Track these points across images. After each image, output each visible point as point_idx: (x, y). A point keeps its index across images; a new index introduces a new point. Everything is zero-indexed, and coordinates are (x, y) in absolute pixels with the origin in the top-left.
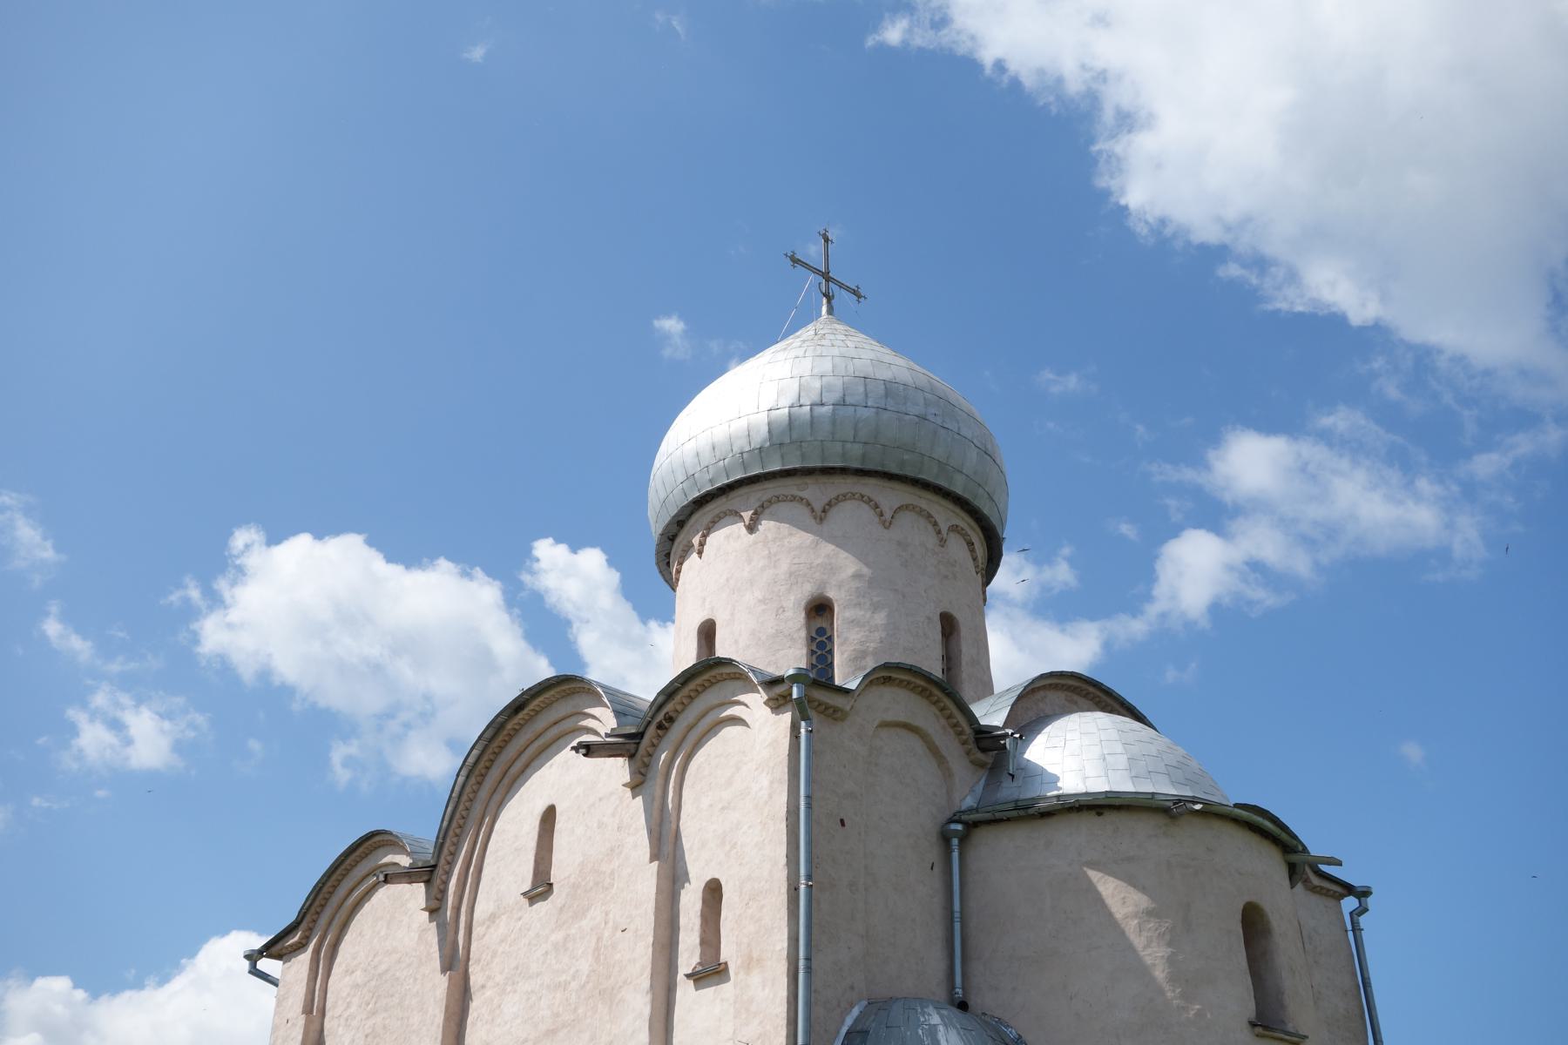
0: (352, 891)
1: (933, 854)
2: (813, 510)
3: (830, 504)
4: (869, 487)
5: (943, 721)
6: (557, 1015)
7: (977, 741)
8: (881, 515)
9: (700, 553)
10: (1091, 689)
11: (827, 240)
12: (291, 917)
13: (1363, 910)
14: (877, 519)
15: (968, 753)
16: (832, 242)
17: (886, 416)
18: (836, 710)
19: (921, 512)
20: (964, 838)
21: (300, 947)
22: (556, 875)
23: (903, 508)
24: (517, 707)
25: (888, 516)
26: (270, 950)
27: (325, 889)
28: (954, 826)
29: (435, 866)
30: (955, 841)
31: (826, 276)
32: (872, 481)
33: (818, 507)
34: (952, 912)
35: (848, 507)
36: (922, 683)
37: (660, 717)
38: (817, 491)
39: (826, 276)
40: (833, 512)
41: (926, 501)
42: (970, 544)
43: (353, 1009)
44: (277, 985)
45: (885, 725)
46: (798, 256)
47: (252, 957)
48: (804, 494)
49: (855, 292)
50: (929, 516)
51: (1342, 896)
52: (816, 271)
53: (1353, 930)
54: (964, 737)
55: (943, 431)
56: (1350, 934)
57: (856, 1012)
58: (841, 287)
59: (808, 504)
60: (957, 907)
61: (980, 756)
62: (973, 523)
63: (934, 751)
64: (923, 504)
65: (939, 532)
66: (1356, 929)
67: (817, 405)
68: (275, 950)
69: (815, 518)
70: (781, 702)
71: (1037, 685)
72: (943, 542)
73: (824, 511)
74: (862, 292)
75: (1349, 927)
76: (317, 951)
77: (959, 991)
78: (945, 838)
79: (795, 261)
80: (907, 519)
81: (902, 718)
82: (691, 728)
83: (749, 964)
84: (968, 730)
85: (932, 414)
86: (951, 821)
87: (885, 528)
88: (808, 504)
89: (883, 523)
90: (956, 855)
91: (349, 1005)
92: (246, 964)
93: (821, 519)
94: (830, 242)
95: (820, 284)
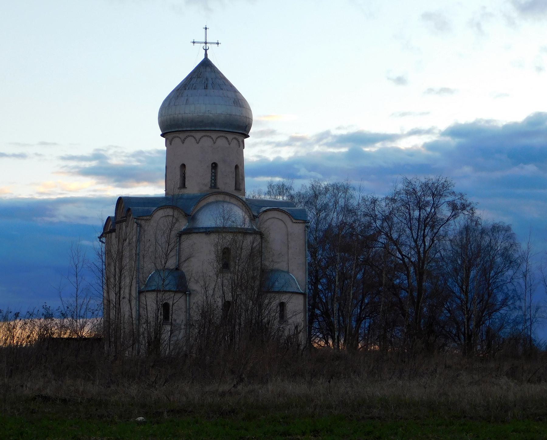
4: (193, 134)
8: (196, 140)
11: (206, 29)
14: (196, 142)
19: (208, 136)
31: (206, 43)
33: (183, 138)
35: (190, 138)
38: (182, 136)
39: (206, 43)
40: (186, 141)
41: (209, 134)
46: (195, 41)
47: (100, 238)
48: (178, 136)
49: (218, 44)
64: (209, 134)
69: (182, 142)
72: (215, 143)
85: (207, 111)
89: (197, 142)
92: (98, 239)
93: (184, 143)
94: (207, 29)
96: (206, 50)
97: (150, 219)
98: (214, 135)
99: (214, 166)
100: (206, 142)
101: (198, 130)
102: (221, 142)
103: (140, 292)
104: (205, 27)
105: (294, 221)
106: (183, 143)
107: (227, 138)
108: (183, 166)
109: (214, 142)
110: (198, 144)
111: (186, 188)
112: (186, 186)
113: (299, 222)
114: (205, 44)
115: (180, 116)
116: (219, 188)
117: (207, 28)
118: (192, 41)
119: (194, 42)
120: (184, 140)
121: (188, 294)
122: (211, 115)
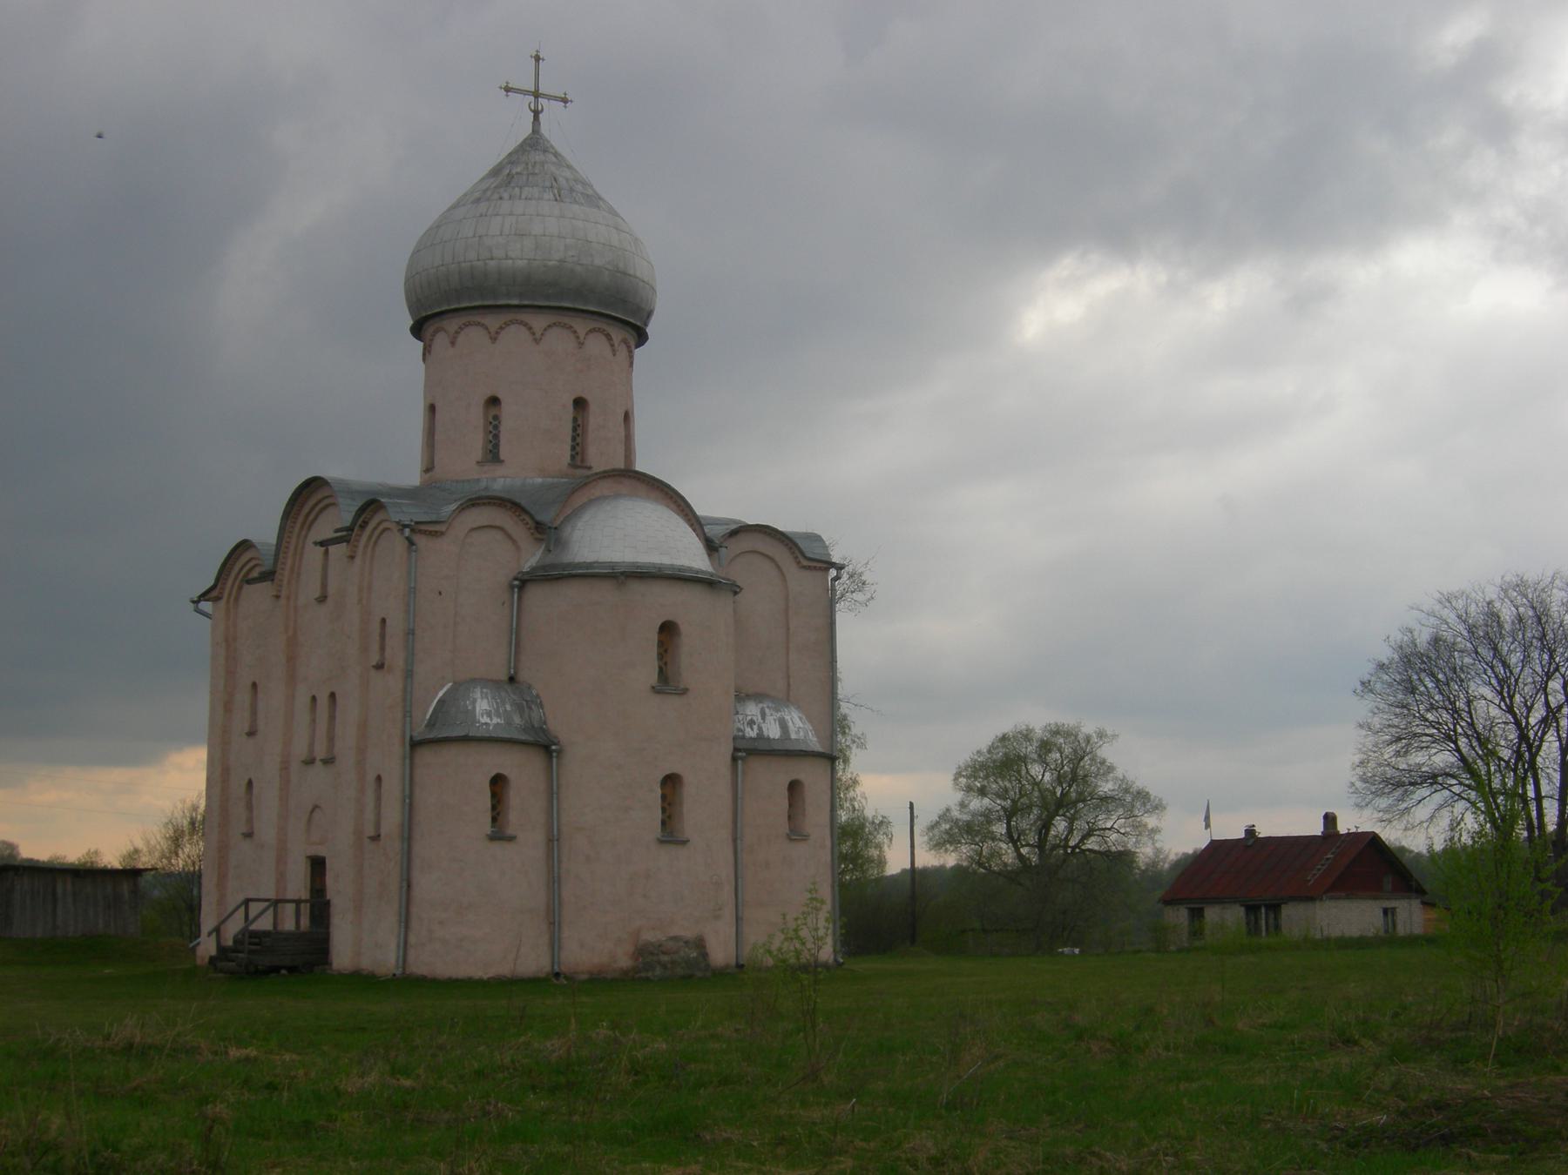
2: (489, 333)
3: (501, 328)
7: (536, 528)
8: (534, 334)
11: (537, 59)
13: (837, 578)
15: (532, 534)
16: (543, 60)
18: (436, 532)
20: (522, 588)
22: (332, 589)
25: (538, 335)
28: (516, 583)
29: (275, 572)
30: (516, 590)
31: (537, 95)
33: (493, 330)
34: (512, 629)
35: (513, 328)
36: (499, 502)
37: (360, 522)
38: (493, 321)
39: (537, 95)
44: (210, 618)
45: (473, 530)
46: (510, 86)
48: (483, 321)
49: (565, 101)
50: (571, 327)
51: (827, 570)
52: (525, 92)
53: (832, 590)
54: (528, 526)
57: (445, 689)
58: (549, 99)
61: (539, 536)
63: (509, 537)
64: (566, 320)
65: (578, 337)
67: (488, 259)
69: (491, 338)
72: (581, 345)
73: (497, 333)
74: (569, 98)
76: (228, 602)
77: (512, 672)
78: (512, 587)
84: (530, 522)
86: (516, 579)
87: (538, 343)
88: (487, 329)
89: (535, 340)
95: (530, 103)
96: (536, 113)
97: (442, 533)
98: (581, 326)
99: (580, 404)
100: (559, 341)
101: (540, 307)
102: (596, 346)
103: (415, 744)
104: (534, 54)
105: (805, 563)
106: (494, 340)
107: (609, 337)
108: (494, 401)
109: (580, 343)
110: (538, 343)
111: (503, 461)
112: (502, 457)
113: (815, 567)
114: (533, 98)
115: (492, 263)
116: (590, 468)
117: (541, 57)
118: (504, 85)
119: (508, 90)
120: (497, 333)
121: (555, 751)
122: (579, 269)
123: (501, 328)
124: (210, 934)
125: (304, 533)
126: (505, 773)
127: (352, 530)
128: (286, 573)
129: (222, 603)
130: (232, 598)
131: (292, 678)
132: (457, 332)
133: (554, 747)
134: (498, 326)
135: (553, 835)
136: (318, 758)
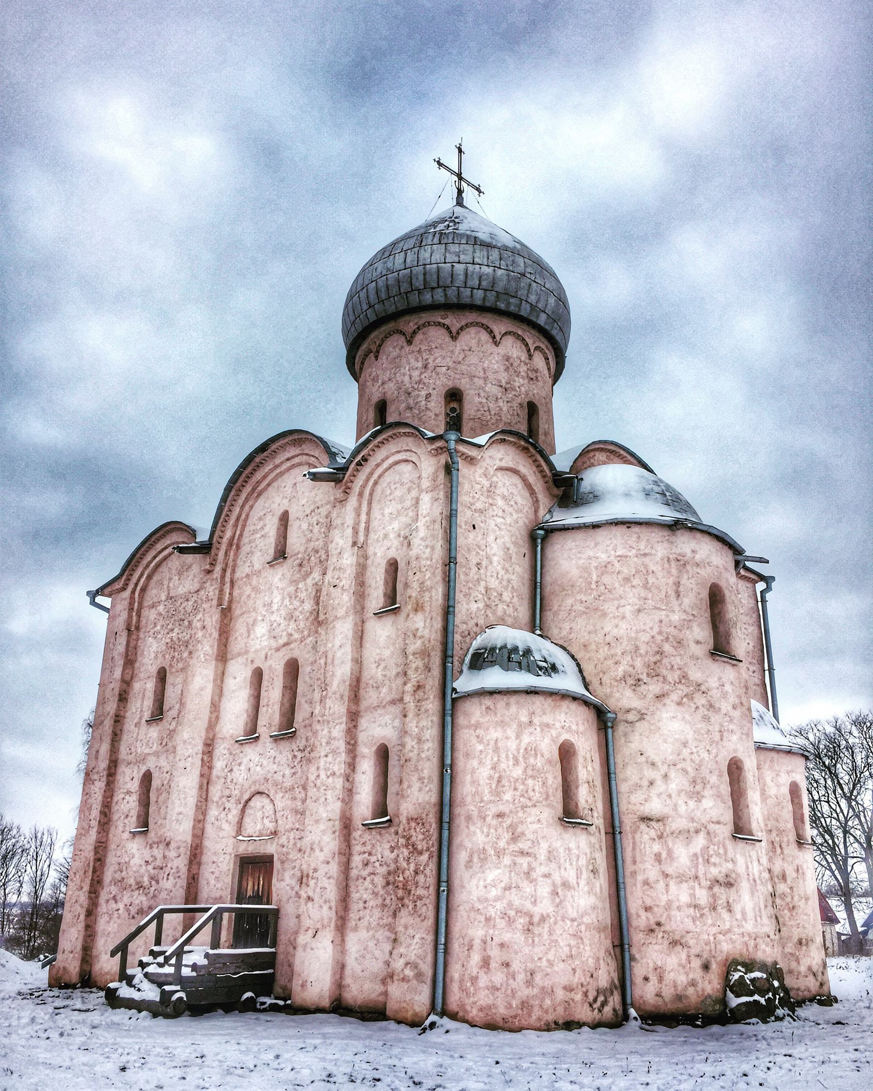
0: (155, 557)
1: (525, 549)
2: (451, 332)
3: (462, 329)
4: (486, 319)
5: (534, 468)
6: (291, 635)
8: (494, 337)
9: (376, 358)
10: (622, 452)
11: (460, 151)
12: (116, 572)
14: (491, 340)
15: (548, 489)
17: (500, 272)
20: (544, 539)
21: (124, 589)
23: (506, 334)
24: (263, 448)
25: (498, 337)
26: (100, 591)
27: (138, 556)
30: (539, 541)
32: (489, 315)
34: (536, 583)
35: (473, 330)
37: (359, 458)
38: (453, 321)
40: (462, 334)
42: (547, 359)
43: (158, 628)
45: (501, 469)
49: (478, 189)
50: (524, 340)
52: (452, 172)
53: (762, 601)
55: (534, 284)
56: (760, 604)
59: (448, 328)
60: (539, 580)
62: (549, 346)
65: (529, 351)
66: (764, 601)
68: (107, 591)
69: (452, 337)
70: (440, 451)
71: (590, 448)
72: (530, 356)
74: (482, 189)
75: (759, 599)
76: (133, 592)
78: (532, 538)
79: (440, 164)
80: (509, 341)
81: (511, 465)
82: (378, 465)
83: (418, 608)
86: (540, 529)
88: (448, 328)
90: (539, 548)
91: (155, 626)
93: (456, 339)
96: (460, 192)
114: (457, 179)
119: (440, 164)
120: (458, 333)
123: (462, 329)
124: (113, 954)
125: (250, 503)
126: (573, 741)
127: (347, 468)
128: (223, 547)
129: (127, 594)
130: (139, 588)
131: (223, 656)
132: (414, 332)
133: (609, 715)
134: (458, 326)
135: (613, 827)
136: (265, 739)
